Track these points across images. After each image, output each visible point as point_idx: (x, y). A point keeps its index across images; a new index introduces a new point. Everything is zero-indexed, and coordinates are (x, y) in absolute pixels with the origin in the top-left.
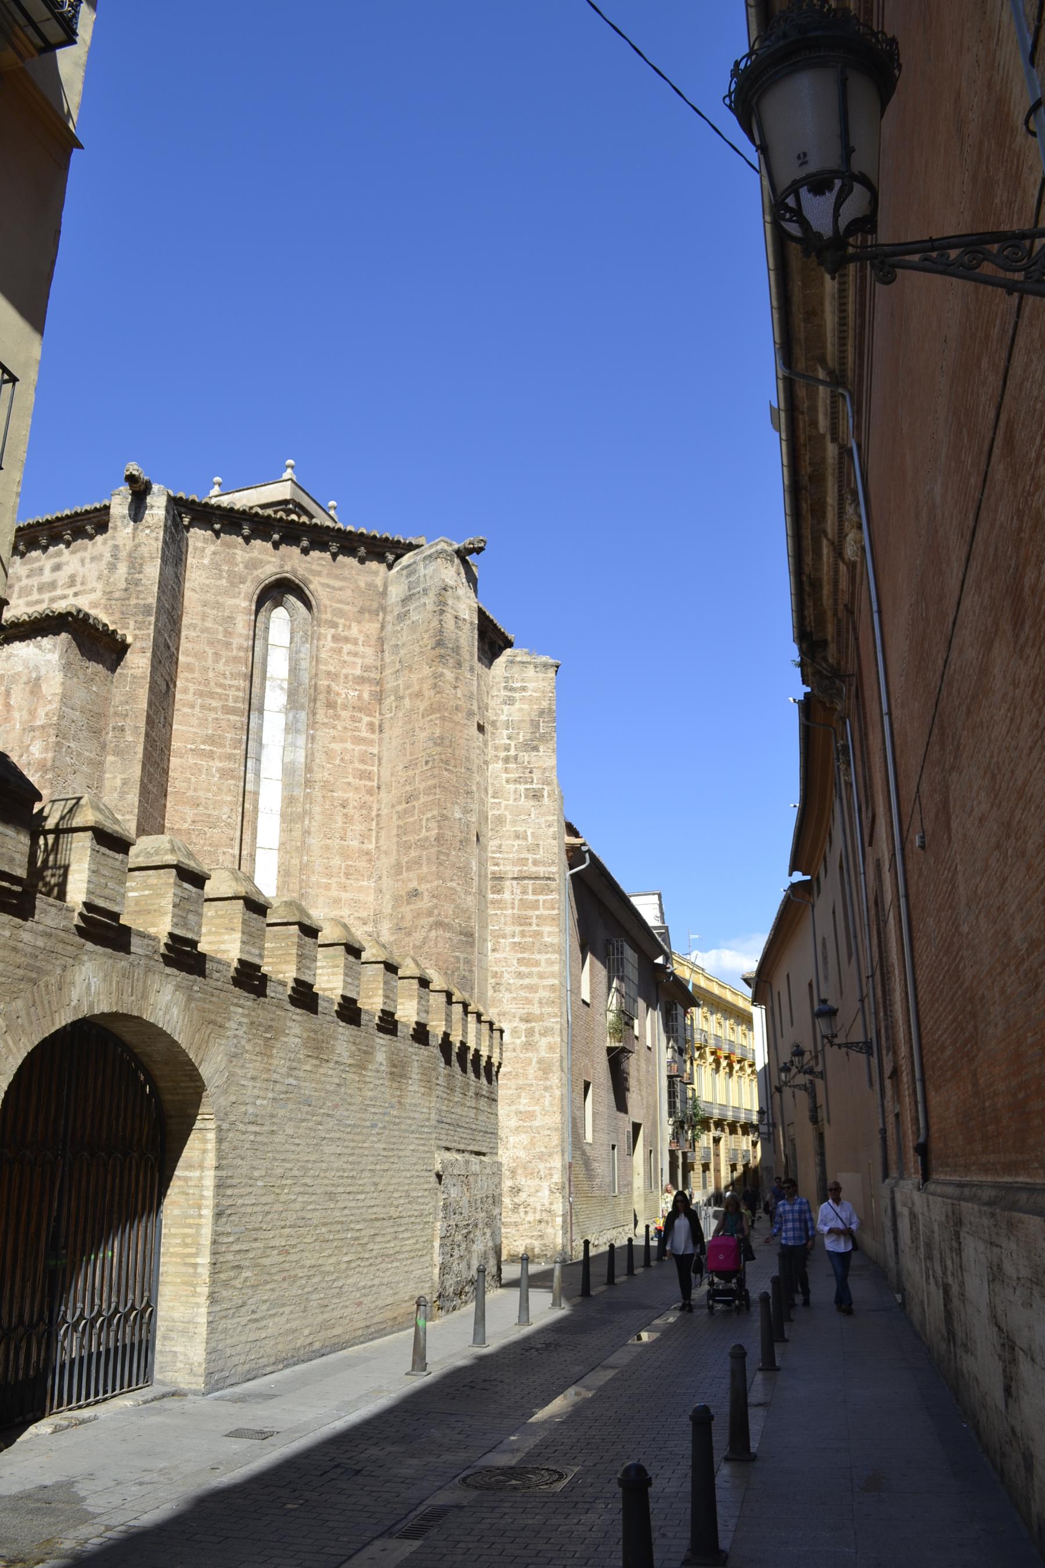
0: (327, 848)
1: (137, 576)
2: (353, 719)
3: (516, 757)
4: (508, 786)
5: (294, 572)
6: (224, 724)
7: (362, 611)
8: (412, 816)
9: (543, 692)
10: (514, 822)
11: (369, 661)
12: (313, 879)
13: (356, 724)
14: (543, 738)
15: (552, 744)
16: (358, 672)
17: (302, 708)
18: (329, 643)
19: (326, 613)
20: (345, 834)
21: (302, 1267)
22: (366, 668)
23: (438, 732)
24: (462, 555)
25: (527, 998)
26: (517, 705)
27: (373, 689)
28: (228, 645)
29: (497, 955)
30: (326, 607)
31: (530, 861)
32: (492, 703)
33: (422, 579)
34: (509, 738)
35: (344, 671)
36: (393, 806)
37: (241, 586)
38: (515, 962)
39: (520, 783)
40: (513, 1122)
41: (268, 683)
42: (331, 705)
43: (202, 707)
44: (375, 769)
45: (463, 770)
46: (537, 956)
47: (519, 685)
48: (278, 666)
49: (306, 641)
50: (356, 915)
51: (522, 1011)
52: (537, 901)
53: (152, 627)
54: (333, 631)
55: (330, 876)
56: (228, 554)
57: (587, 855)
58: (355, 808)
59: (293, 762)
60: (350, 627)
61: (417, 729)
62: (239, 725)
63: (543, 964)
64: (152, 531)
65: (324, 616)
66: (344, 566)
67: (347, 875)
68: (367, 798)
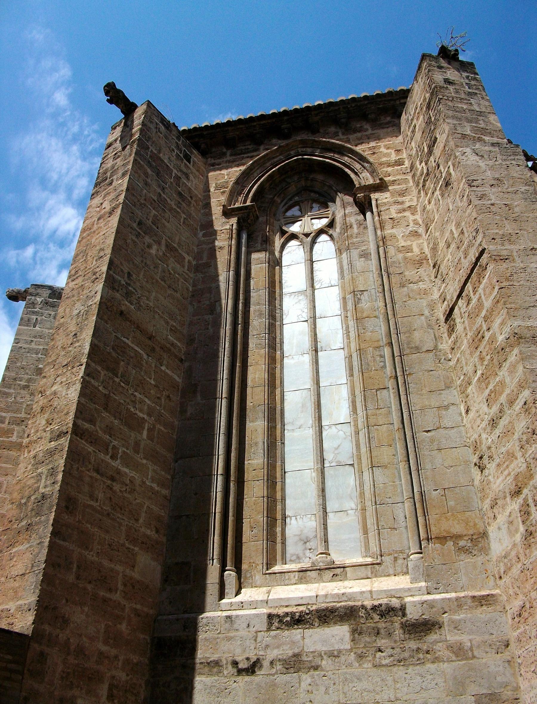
29: (472, 414)
31: (462, 258)
34: (421, 162)
45: (94, 263)
51: (510, 479)
63: (508, 380)
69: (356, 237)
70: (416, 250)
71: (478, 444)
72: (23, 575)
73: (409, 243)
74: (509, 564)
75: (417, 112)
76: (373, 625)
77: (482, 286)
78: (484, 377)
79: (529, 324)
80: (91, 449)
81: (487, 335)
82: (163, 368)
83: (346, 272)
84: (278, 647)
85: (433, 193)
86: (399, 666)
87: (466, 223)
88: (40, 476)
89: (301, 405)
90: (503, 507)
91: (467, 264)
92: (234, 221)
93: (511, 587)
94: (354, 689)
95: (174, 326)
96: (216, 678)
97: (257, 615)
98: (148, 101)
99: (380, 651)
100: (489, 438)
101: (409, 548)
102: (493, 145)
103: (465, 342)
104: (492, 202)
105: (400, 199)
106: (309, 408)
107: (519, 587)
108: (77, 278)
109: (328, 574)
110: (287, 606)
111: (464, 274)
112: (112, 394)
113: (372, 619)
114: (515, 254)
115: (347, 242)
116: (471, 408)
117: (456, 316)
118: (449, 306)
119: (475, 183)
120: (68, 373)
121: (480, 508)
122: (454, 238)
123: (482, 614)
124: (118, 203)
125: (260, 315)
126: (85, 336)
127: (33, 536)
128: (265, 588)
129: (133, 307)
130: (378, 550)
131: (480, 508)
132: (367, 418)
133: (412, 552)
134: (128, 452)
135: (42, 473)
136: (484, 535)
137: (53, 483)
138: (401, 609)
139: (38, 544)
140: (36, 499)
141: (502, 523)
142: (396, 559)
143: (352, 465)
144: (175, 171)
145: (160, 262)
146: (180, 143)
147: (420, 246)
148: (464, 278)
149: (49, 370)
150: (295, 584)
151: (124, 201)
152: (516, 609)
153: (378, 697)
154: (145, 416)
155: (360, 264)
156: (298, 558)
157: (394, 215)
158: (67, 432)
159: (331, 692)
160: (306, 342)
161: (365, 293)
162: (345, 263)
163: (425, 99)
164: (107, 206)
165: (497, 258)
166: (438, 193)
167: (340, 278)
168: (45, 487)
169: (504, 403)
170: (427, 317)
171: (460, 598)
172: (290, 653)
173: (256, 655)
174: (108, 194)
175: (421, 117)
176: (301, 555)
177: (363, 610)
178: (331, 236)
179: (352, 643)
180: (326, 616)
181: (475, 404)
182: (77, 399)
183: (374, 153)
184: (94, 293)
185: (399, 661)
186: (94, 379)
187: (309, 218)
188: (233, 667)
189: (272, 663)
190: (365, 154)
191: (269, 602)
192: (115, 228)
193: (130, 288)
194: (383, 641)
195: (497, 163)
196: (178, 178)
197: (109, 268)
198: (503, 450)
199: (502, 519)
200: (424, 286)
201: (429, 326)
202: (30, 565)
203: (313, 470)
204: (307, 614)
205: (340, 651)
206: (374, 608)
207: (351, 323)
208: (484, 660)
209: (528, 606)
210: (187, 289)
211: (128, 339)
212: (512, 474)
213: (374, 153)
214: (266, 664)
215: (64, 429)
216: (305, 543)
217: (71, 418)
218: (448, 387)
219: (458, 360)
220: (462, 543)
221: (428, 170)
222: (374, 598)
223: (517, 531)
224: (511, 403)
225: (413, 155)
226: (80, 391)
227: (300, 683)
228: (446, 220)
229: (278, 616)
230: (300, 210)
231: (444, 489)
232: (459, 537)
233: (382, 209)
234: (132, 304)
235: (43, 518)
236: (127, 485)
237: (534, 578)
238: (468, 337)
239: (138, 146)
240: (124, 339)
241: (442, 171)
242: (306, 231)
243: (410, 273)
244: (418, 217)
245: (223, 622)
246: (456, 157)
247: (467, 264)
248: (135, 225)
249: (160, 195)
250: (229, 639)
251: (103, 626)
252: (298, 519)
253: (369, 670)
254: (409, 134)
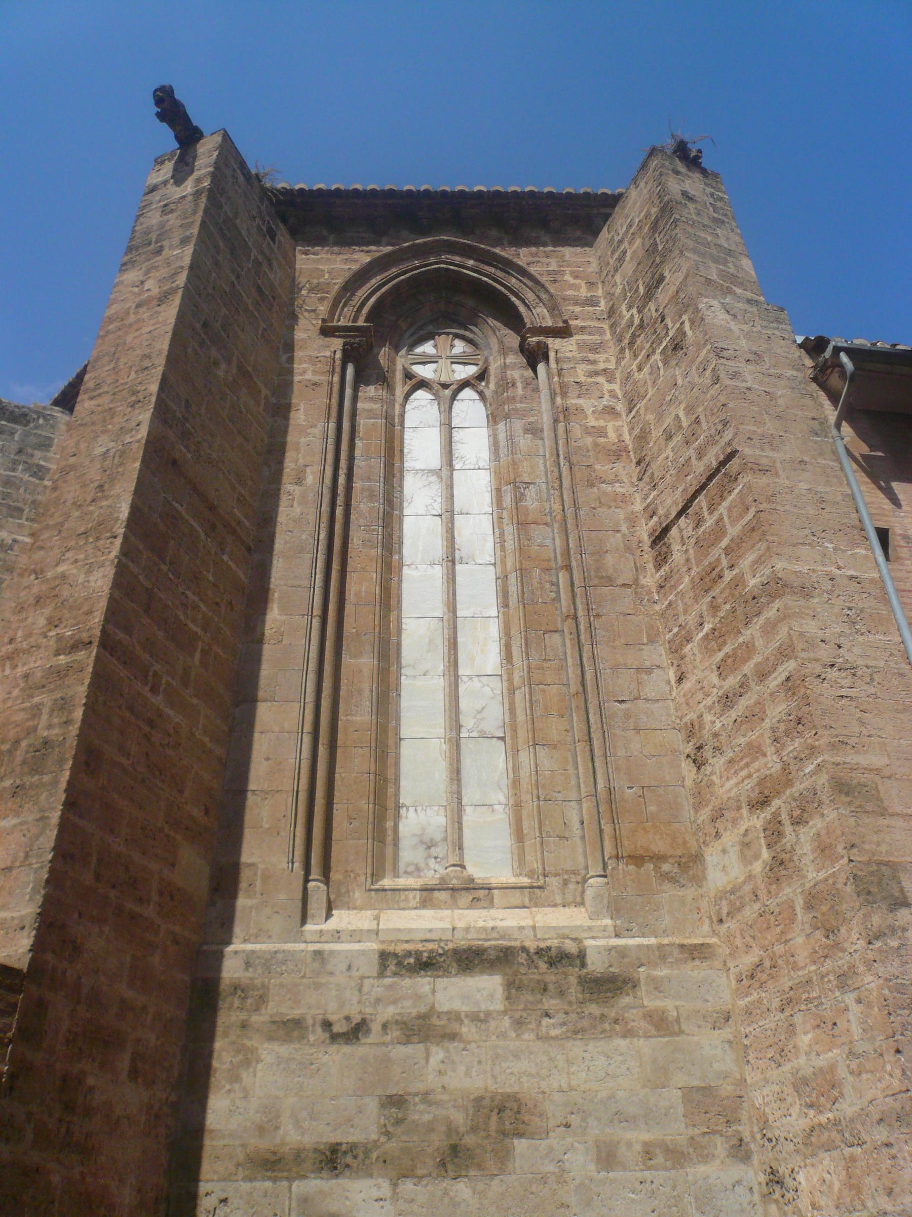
3: (641, 326)
10: (660, 417)
14: (665, 256)
25: (750, 745)
26: (629, 254)
29: (687, 685)
31: (693, 458)
34: (630, 307)
39: (654, 352)
40: (795, 1121)
45: (133, 375)
47: (624, 229)
51: (749, 784)
52: (721, 519)
57: (844, 358)
63: (759, 643)
69: (521, 402)
70: (612, 436)
71: (696, 728)
72: (9, 869)
73: (602, 423)
74: (738, 903)
75: (632, 231)
76: (537, 977)
77: (725, 504)
78: (716, 633)
79: (797, 568)
80: (124, 673)
81: (728, 576)
82: (225, 558)
83: (503, 452)
84: (395, 1002)
85: (648, 356)
86: (574, 1039)
87: (705, 409)
88: (38, 709)
89: (427, 641)
90: (735, 822)
91: (702, 469)
92: (337, 344)
93: (738, 935)
94: (509, 1071)
95: (242, 495)
96: (297, 1046)
97: (363, 953)
98: (225, 131)
99: (548, 1015)
100: (717, 721)
101: (587, 868)
102: (749, 301)
103: (687, 579)
104: (749, 385)
105: (591, 356)
106: (441, 647)
107: (753, 937)
108: (100, 395)
109: (465, 898)
110: (407, 942)
111: (695, 483)
112: (156, 590)
113: (536, 967)
114: (778, 465)
115: (506, 407)
116: (688, 676)
117: (672, 541)
118: (661, 524)
119: (725, 354)
120: (90, 548)
121: (692, 819)
122: (681, 427)
123: (695, 971)
124: (174, 285)
125: (372, 497)
126: (119, 491)
127: (26, 806)
128: (369, 912)
129: (189, 456)
130: (540, 867)
131: (692, 819)
132: (529, 672)
133: (591, 874)
134: (174, 683)
135: (41, 704)
136: (697, 858)
137: (65, 723)
138: (578, 956)
139: (38, 820)
140: (30, 745)
141: (730, 844)
142: (566, 883)
143: (502, 739)
144: (254, 252)
145: (229, 392)
146: (263, 208)
147: (619, 430)
148: (694, 488)
149: (50, 538)
150: (416, 908)
151: (186, 284)
152: (746, 968)
153: (544, 1085)
154: (199, 630)
155: (524, 442)
156: (418, 869)
157: (582, 379)
158: (90, 643)
159: (474, 1074)
160: (438, 548)
161: (531, 487)
162: (502, 436)
163: (647, 216)
164: (152, 286)
165: (755, 467)
166: (657, 357)
167: (493, 458)
168: (50, 727)
169: (749, 674)
170: (624, 535)
171: (664, 945)
172: (414, 1012)
173: (360, 1012)
174: (156, 268)
175: (638, 242)
176: (422, 865)
177: (524, 955)
178: (481, 394)
179: (506, 1002)
180: (469, 959)
181: (695, 671)
182: (107, 591)
183: (555, 281)
184: (134, 424)
185: (576, 1032)
186: (133, 561)
187: (449, 361)
188: (324, 1031)
189: (385, 1026)
190: (543, 279)
191: (380, 934)
192: (172, 326)
193: (187, 425)
194: (553, 1002)
195: (755, 329)
196: (258, 263)
197: (161, 388)
198: (742, 740)
199: (730, 838)
200: (621, 490)
201: (628, 549)
202: (22, 855)
203: (443, 740)
204: (440, 955)
205: (488, 1014)
206: (539, 952)
207: (509, 530)
208: (696, 1039)
209: (767, 964)
210: (263, 440)
211: (182, 506)
212: (754, 776)
213: (555, 281)
214: (376, 1027)
215: (85, 636)
216: (429, 848)
217: (97, 620)
218: (651, 641)
219: (670, 604)
220: (666, 867)
221: (642, 320)
222: (539, 936)
223: (757, 857)
224: (762, 675)
225: (616, 295)
226: (114, 580)
227: (427, 1059)
228: (668, 398)
229: (395, 955)
230: (435, 346)
231: (643, 787)
232: (660, 858)
233: (565, 366)
234: (189, 451)
235: (46, 778)
236: (169, 735)
237: (782, 926)
238: (693, 573)
239: (209, 199)
240: (176, 505)
241: (670, 327)
242: (444, 379)
243: (602, 468)
244: (616, 387)
245: (309, 960)
246: (697, 310)
247: (700, 468)
248: (198, 326)
249: (234, 286)
250: (318, 986)
251: (128, 958)
252: (419, 811)
253: (531, 1043)
254: (612, 262)
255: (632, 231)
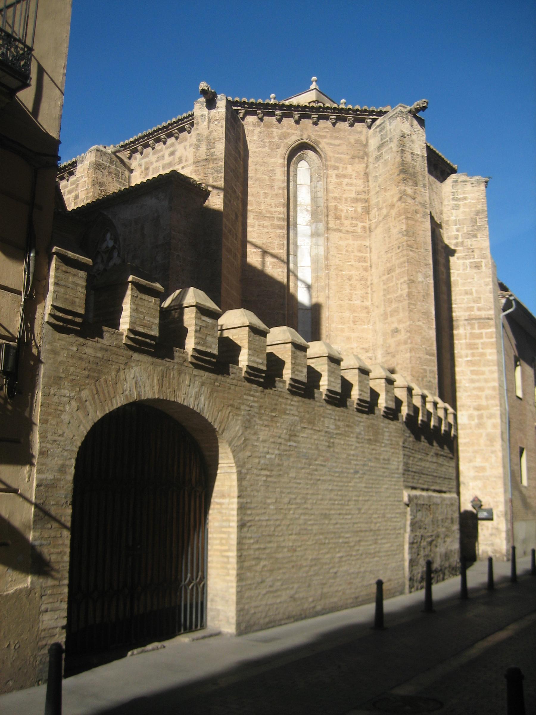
0: (341, 306)
1: (213, 150)
2: (352, 225)
3: (462, 243)
4: (458, 261)
5: (309, 138)
6: (272, 235)
7: (353, 158)
8: (392, 282)
9: (478, 199)
10: (464, 284)
11: (360, 188)
12: (333, 326)
13: (354, 228)
14: (479, 228)
15: (486, 232)
16: (353, 195)
17: (320, 221)
18: (334, 179)
19: (331, 160)
20: (351, 297)
21: (306, 559)
22: (359, 193)
23: (404, 227)
24: (415, 114)
26: (462, 209)
27: (364, 205)
28: (272, 187)
30: (330, 157)
31: (475, 309)
32: (445, 210)
33: (389, 132)
34: (458, 231)
35: (345, 196)
36: (380, 277)
37: (278, 150)
38: (469, 373)
39: (466, 259)
40: (472, 473)
41: (299, 208)
42: (338, 218)
43: (259, 226)
44: (368, 255)
45: (423, 251)
46: (483, 369)
47: (461, 196)
48: (304, 197)
49: (320, 180)
50: (362, 346)
51: (475, 404)
52: (481, 333)
53: (223, 179)
54: (336, 172)
55: (343, 323)
56: (268, 131)
57: (513, 303)
58: (357, 280)
59: (317, 255)
60: (346, 168)
61: (392, 227)
62: (282, 235)
64: (219, 122)
65: (329, 163)
66: (340, 130)
67: (354, 322)
68: (364, 273)
224: (486, 381)
241: (476, 257)
255: (465, 202)
